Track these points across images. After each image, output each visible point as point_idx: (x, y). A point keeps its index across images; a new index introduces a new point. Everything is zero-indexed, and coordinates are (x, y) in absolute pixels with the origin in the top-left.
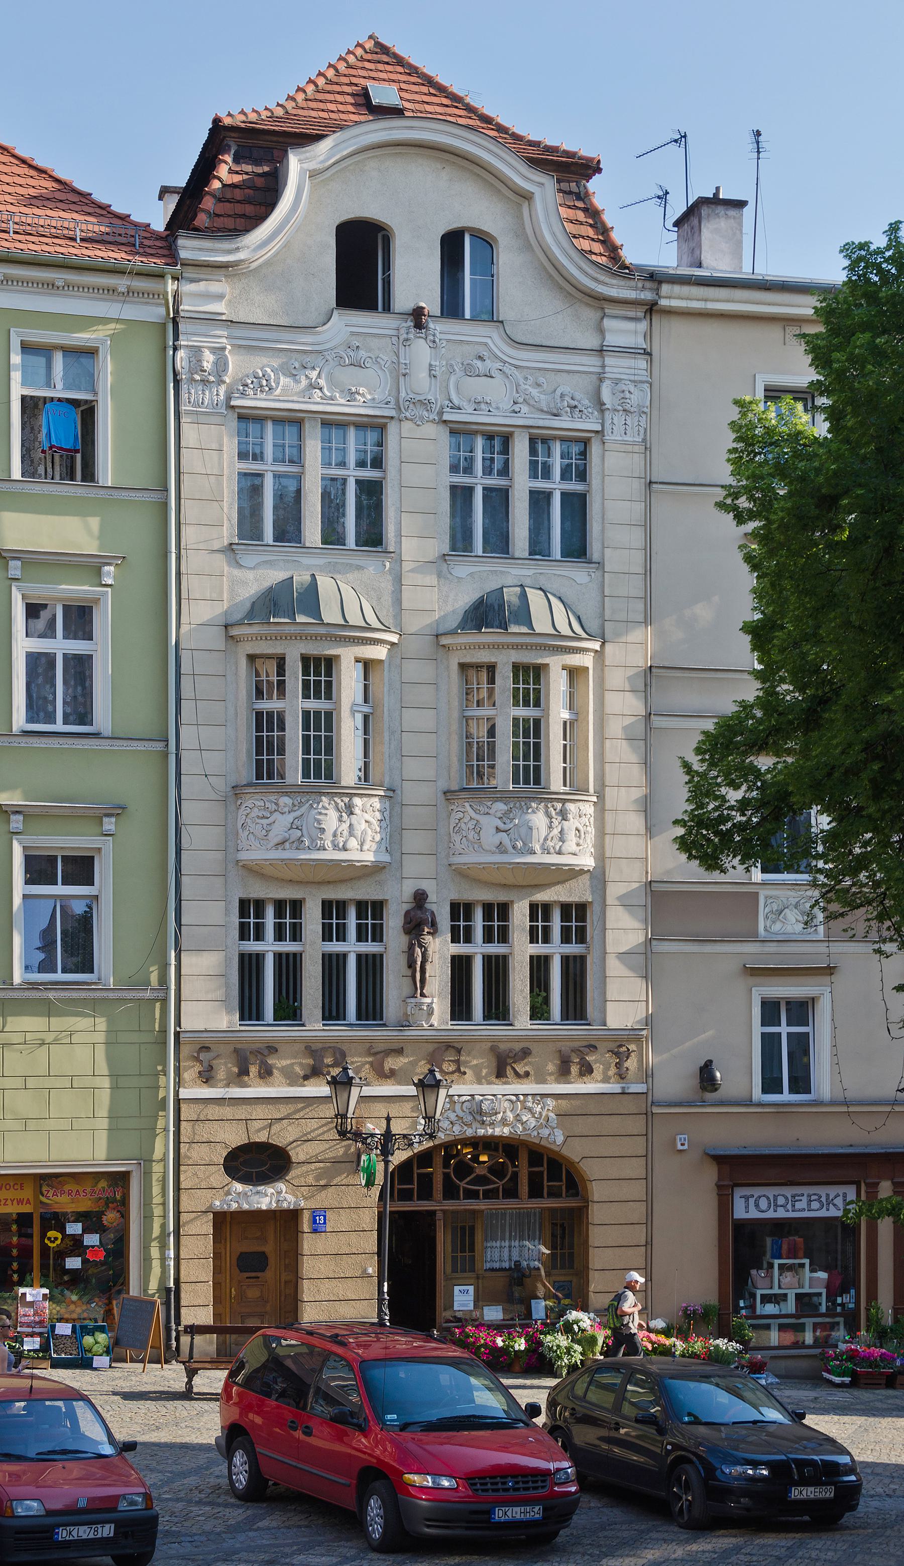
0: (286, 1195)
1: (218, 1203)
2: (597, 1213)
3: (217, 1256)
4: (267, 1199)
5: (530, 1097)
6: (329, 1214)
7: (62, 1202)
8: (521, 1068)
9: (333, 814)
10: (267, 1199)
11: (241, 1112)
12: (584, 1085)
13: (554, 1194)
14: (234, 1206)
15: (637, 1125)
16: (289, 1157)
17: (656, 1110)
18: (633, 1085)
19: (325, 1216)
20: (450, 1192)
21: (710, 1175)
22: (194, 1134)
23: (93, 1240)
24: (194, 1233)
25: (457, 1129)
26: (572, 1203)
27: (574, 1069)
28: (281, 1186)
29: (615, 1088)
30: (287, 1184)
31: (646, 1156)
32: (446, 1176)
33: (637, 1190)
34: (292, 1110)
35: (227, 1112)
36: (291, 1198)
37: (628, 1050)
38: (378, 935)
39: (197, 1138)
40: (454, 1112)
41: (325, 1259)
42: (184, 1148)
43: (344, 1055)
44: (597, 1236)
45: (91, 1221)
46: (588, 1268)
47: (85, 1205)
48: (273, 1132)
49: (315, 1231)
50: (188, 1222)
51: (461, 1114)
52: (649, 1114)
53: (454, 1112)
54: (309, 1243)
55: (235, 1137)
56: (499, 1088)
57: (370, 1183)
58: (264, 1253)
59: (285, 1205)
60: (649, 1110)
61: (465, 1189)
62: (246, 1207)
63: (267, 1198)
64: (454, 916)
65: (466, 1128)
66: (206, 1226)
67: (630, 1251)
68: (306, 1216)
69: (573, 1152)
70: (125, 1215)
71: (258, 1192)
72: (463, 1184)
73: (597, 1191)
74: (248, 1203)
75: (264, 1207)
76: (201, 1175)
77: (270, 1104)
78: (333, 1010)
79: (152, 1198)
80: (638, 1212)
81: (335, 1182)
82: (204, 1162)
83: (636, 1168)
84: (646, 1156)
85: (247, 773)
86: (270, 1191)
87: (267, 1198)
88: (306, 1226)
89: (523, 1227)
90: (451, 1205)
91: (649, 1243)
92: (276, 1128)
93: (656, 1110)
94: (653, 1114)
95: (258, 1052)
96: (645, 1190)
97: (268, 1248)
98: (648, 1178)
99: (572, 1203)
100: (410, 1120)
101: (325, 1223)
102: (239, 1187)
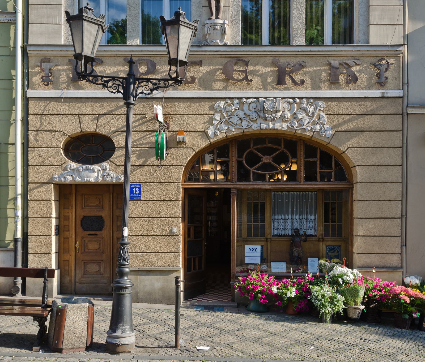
0: (110, 172)
1: (56, 176)
2: (359, 192)
4: (95, 175)
5: (305, 100)
6: (142, 187)
10: (95, 175)
11: (75, 108)
12: (350, 91)
14: (69, 179)
15: (396, 123)
16: (113, 143)
17: (410, 111)
18: (391, 91)
19: (140, 189)
22: (41, 125)
24: (38, 198)
25: (245, 124)
26: (340, 185)
27: (342, 78)
28: (106, 164)
29: (377, 93)
30: (110, 163)
31: (402, 147)
32: (240, 164)
33: (395, 174)
34: (115, 107)
35: (63, 107)
36: (113, 174)
37: (388, 63)
39: (43, 128)
40: (243, 110)
41: (140, 220)
42: (31, 136)
43: (154, 65)
46: (353, 235)
48: (99, 124)
49: (132, 199)
50: (33, 189)
51: (248, 112)
52: (405, 114)
53: (243, 110)
54: (132, 209)
56: (279, 93)
58: (101, 217)
59: (109, 179)
60: (405, 111)
61: (254, 173)
62: (78, 179)
63: (94, 174)
65: (252, 123)
66: (51, 193)
67: (387, 222)
71: (87, 169)
72: (252, 170)
74: (80, 177)
75: (92, 180)
76: (43, 154)
77: (97, 104)
79: (8, 171)
80: (395, 191)
81: (148, 163)
82: (47, 146)
83: (394, 156)
84: (402, 147)
86: (96, 167)
87: (94, 174)
90: (242, 185)
91: (404, 216)
92: (102, 120)
93: (410, 111)
94: (408, 114)
96: (400, 174)
97: (105, 214)
98: (403, 166)
99: (340, 185)
100: (208, 117)
101: (140, 193)
102: (74, 165)
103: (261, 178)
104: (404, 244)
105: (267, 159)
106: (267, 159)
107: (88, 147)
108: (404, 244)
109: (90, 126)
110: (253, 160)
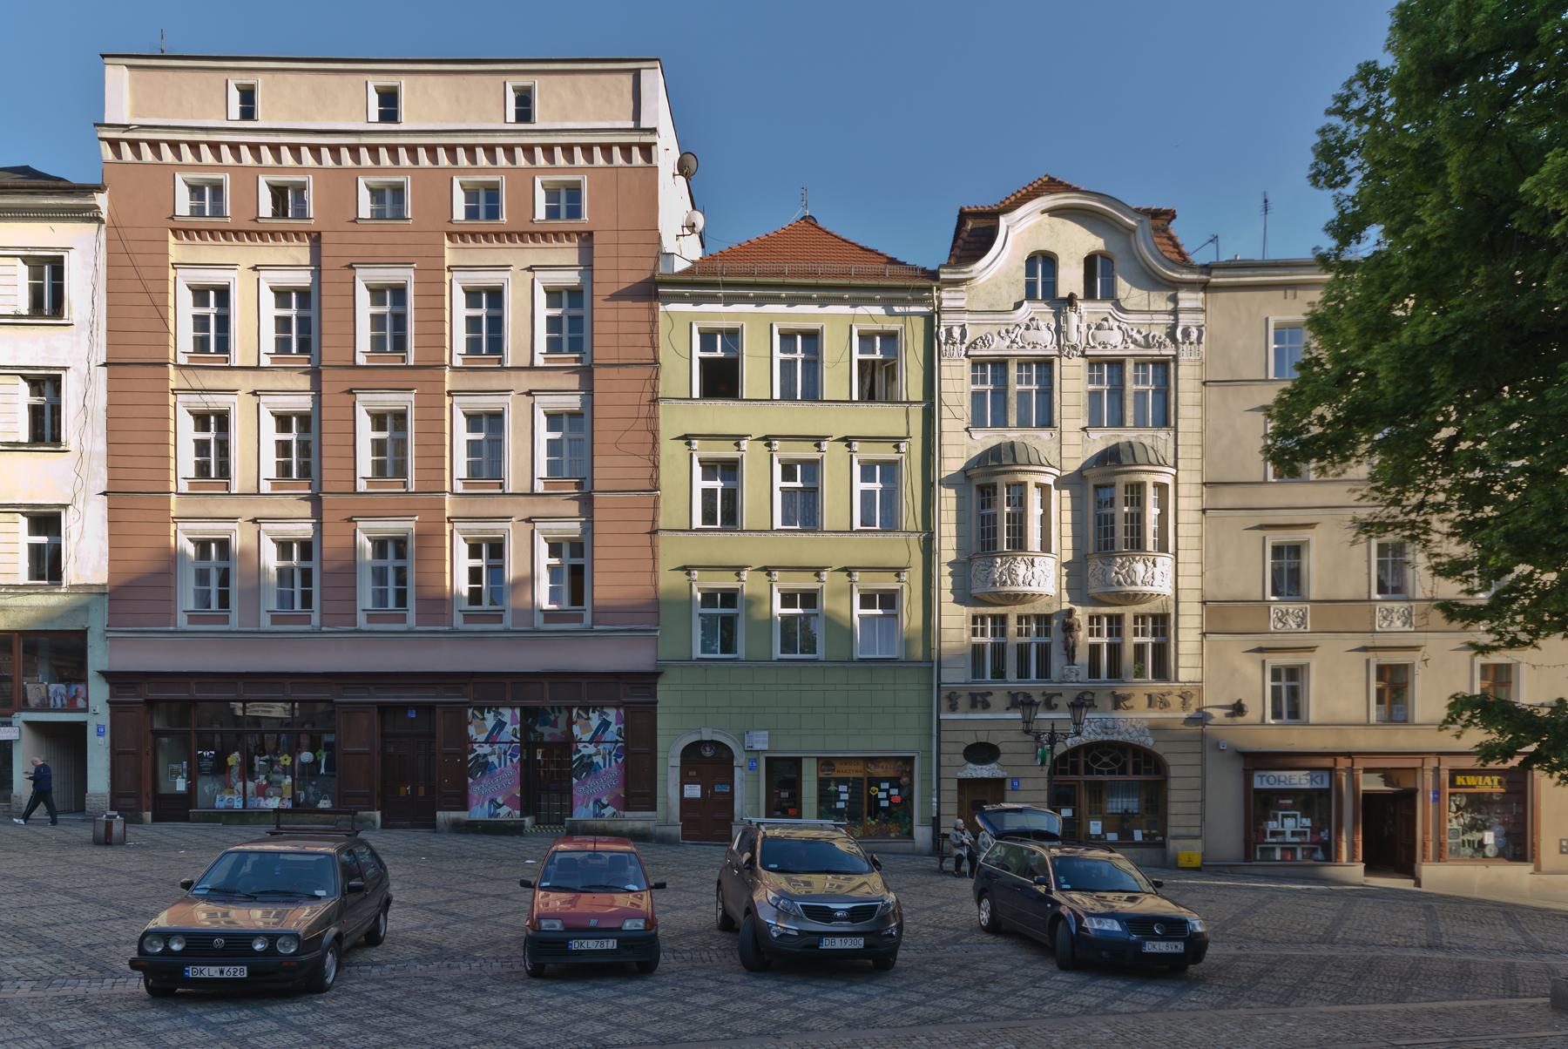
2: (1173, 783)
3: (960, 801)
7: (879, 771)
8: (1128, 703)
9: (1023, 566)
13: (1147, 772)
20: (1089, 771)
21: (1238, 765)
23: (894, 792)
26: (1157, 778)
33: (1196, 771)
38: (1048, 633)
44: (1173, 796)
45: (895, 782)
47: (891, 773)
55: (970, 739)
57: (1043, 764)
64: (1091, 622)
66: (955, 786)
68: (1008, 783)
69: (1159, 749)
70: (912, 780)
73: (1173, 772)
78: (1023, 673)
80: (1196, 783)
85: (976, 548)
88: (1008, 785)
89: (1128, 789)
90: (1089, 778)
91: (1203, 801)
95: (982, 695)
99: (1157, 778)
103: (1102, 773)
104: (1203, 819)
105: (1105, 759)
106: (1105, 759)
107: (982, 752)
108: (1203, 819)
109: (983, 738)
110: (1095, 760)
